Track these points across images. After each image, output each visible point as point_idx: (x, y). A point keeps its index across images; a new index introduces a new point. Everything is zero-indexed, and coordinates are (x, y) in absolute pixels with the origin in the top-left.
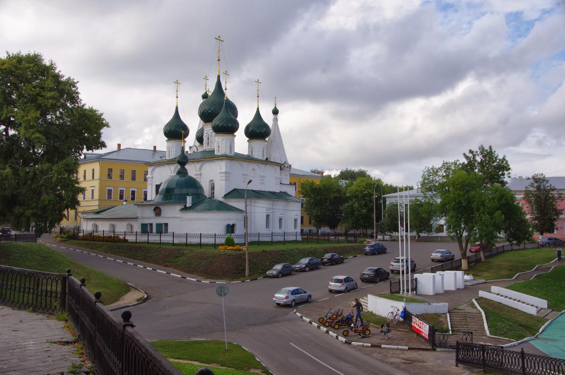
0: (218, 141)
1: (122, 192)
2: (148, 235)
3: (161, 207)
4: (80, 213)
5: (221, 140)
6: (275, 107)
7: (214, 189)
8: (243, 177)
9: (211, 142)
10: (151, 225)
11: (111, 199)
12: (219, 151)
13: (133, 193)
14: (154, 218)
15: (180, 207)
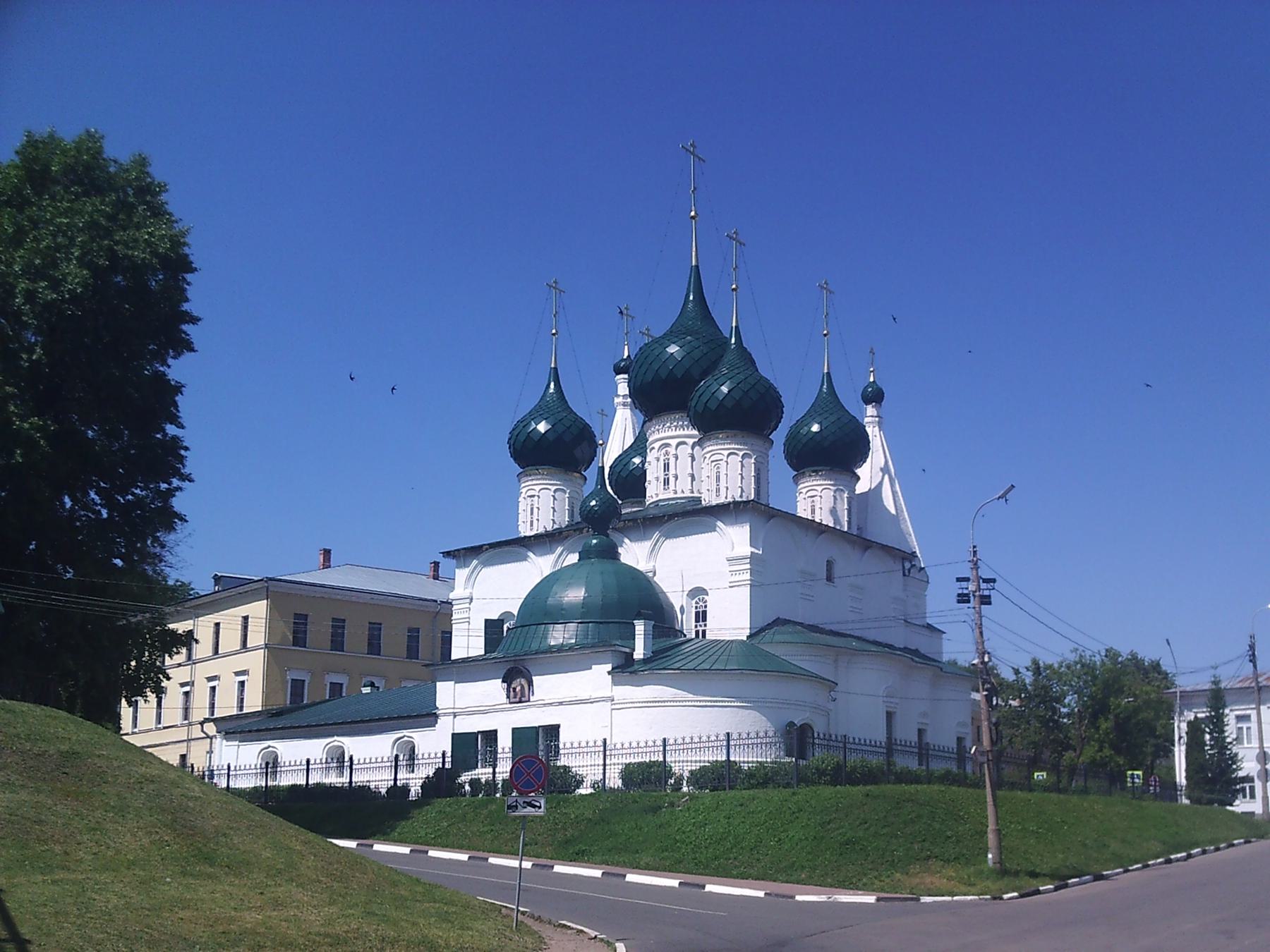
0: (714, 458)
5: (726, 453)
7: (704, 619)
9: (676, 477)
10: (491, 736)
12: (718, 490)
14: (502, 710)
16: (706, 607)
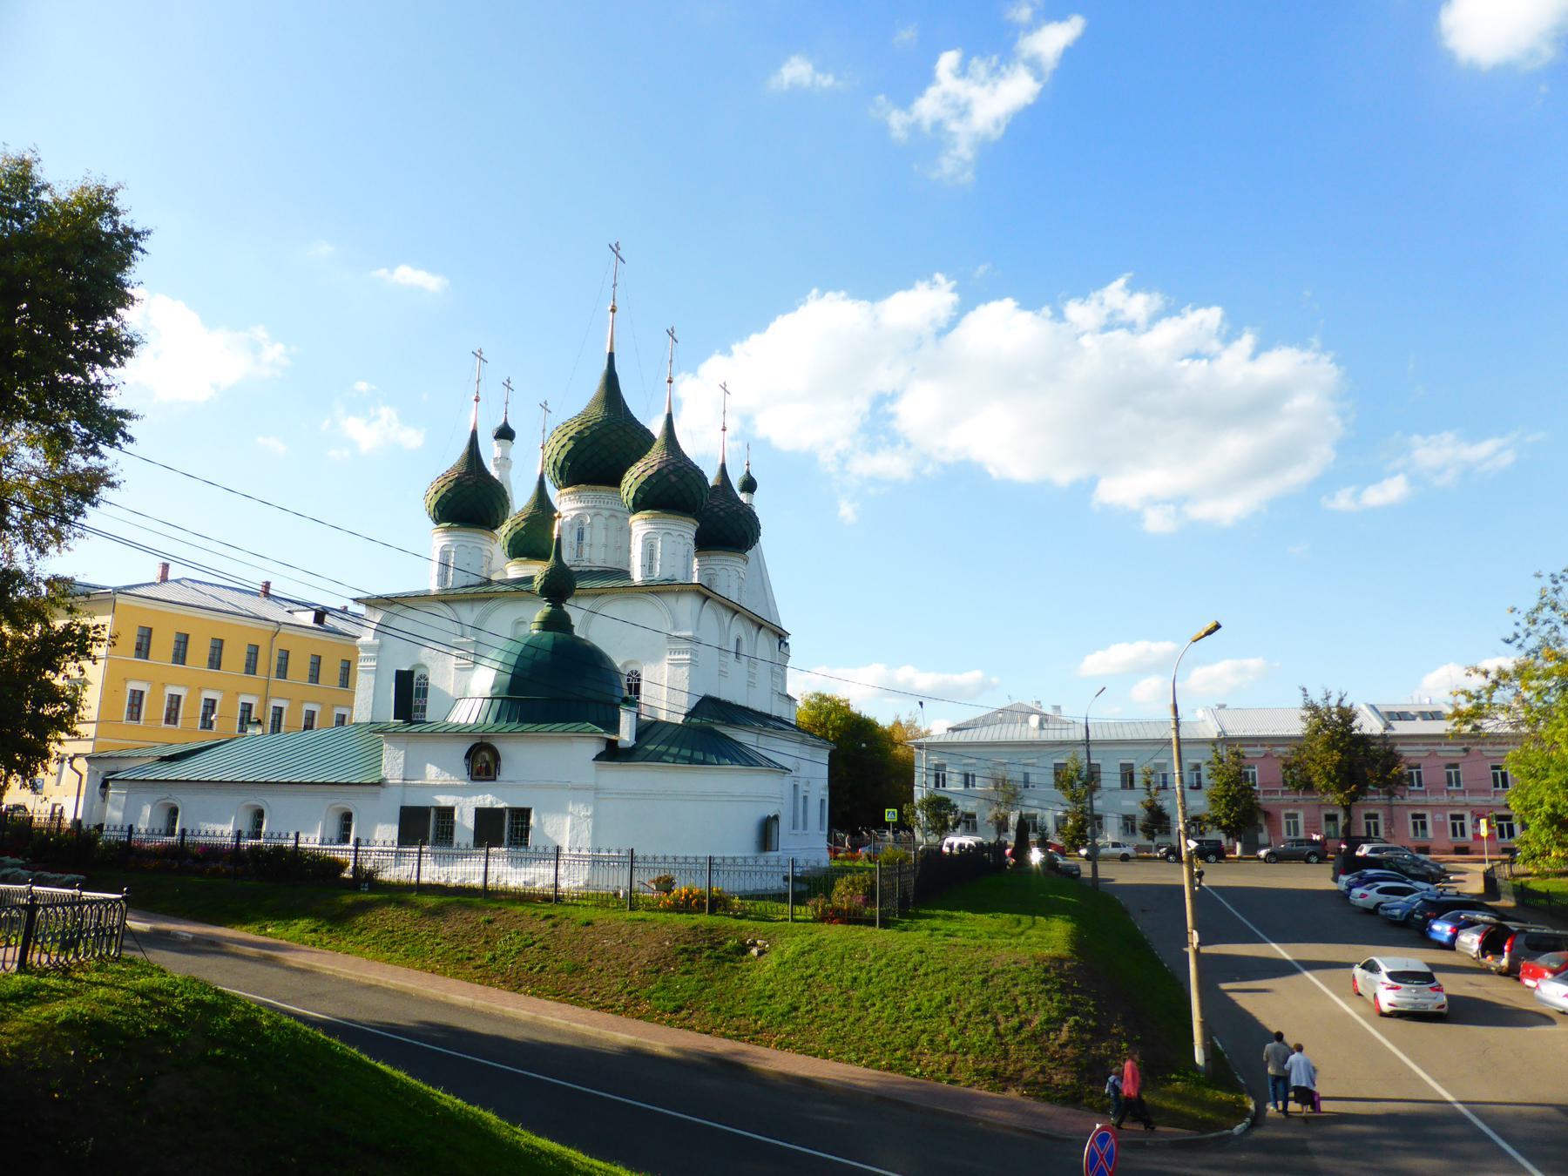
1: (175, 700)
2: (488, 855)
3: (504, 748)
4: (83, 759)
6: (748, 472)
8: (722, 658)
10: (446, 814)
11: (138, 719)
13: (210, 705)
15: (595, 747)
16: (639, 680)
